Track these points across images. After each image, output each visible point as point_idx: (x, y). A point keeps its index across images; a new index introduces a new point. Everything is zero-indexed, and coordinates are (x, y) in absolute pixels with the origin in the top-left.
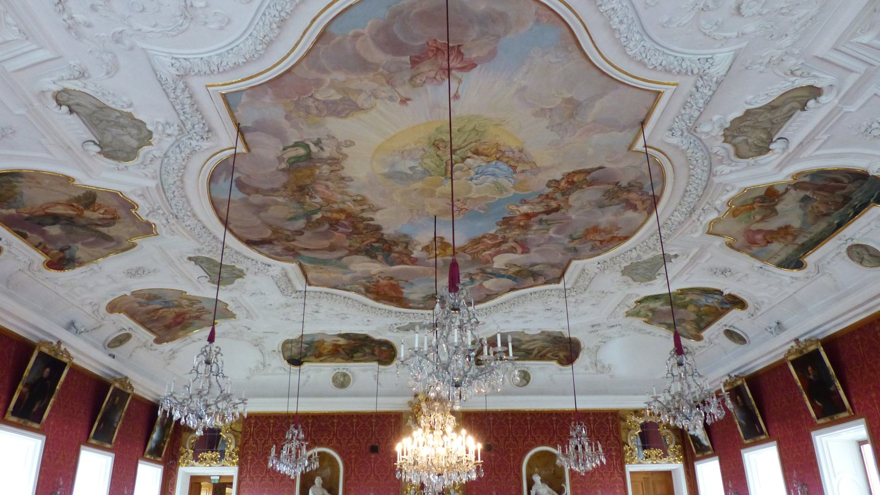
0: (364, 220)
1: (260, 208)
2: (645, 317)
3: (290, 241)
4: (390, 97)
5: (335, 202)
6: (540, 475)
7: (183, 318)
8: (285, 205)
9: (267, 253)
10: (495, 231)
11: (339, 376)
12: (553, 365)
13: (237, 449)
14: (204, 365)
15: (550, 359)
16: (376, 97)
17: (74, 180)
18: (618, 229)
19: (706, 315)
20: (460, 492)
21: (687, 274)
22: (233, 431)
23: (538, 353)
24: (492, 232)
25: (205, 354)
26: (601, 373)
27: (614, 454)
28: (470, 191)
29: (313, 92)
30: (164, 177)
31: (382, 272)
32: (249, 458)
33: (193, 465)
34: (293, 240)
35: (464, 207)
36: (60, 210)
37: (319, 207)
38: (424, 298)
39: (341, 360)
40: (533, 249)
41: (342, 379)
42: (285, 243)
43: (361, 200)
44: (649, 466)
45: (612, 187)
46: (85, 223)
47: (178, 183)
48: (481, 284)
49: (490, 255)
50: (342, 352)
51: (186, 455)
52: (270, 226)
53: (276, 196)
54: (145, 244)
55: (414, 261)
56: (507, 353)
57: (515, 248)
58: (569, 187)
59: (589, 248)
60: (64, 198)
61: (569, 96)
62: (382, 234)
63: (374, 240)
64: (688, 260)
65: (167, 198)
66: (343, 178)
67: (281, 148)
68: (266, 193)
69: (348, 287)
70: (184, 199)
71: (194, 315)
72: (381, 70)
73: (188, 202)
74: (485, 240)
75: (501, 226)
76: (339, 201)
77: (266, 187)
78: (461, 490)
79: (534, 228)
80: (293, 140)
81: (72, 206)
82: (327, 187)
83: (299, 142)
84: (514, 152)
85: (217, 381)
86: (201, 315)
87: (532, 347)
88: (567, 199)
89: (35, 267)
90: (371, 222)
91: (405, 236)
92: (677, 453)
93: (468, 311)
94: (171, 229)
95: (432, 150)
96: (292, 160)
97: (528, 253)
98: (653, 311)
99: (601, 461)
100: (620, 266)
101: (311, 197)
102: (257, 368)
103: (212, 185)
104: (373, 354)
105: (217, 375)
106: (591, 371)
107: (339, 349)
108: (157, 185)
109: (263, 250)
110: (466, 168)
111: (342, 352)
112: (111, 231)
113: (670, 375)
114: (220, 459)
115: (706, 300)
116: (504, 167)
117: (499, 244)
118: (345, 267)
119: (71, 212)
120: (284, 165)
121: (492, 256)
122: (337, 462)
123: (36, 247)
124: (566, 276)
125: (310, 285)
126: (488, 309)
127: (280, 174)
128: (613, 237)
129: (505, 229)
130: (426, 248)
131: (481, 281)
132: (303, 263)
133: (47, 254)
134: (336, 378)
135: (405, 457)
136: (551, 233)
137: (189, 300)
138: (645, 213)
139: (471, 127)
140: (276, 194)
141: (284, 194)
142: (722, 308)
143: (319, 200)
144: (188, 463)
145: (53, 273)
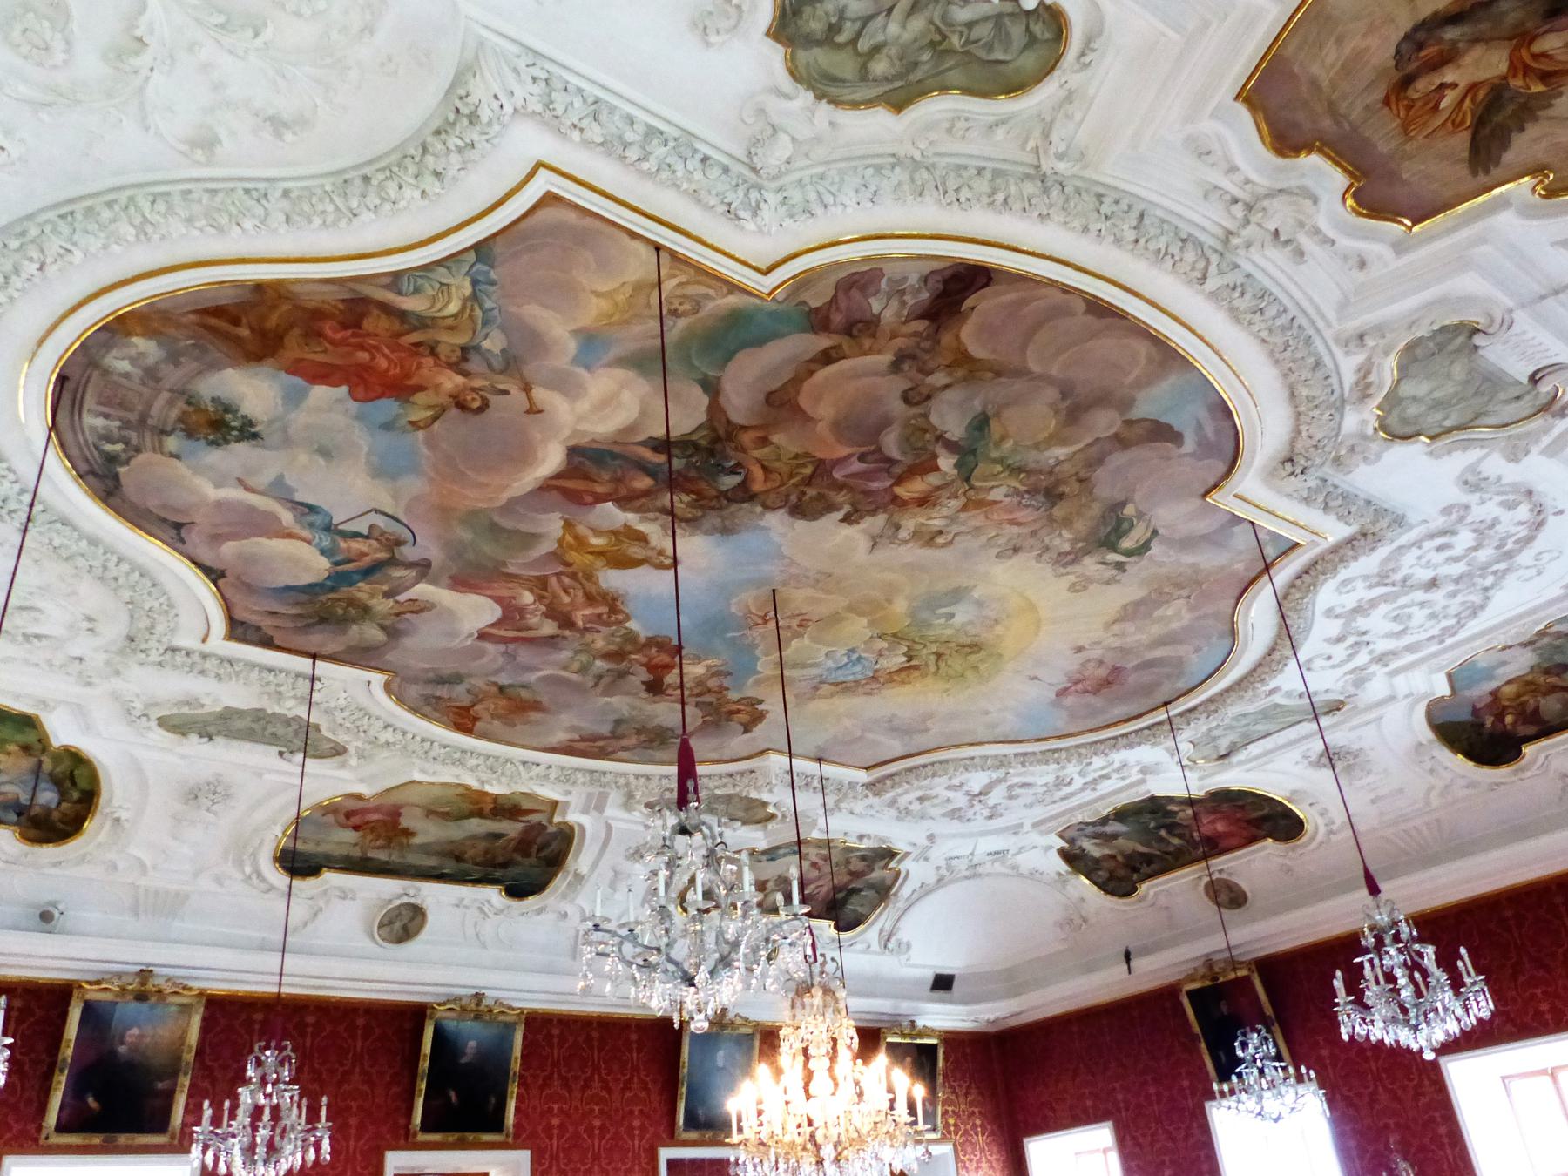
1: (1074, 409)
34: (896, 367)
42: (899, 342)
53: (1075, 453)
67: (1161, 531)
76: (962, 515)
80: (1156, 549)
90: (840, 515)
96: (1126, 525)
120: (1129, 510)
127: (1119, 497)
143: (995, 495)
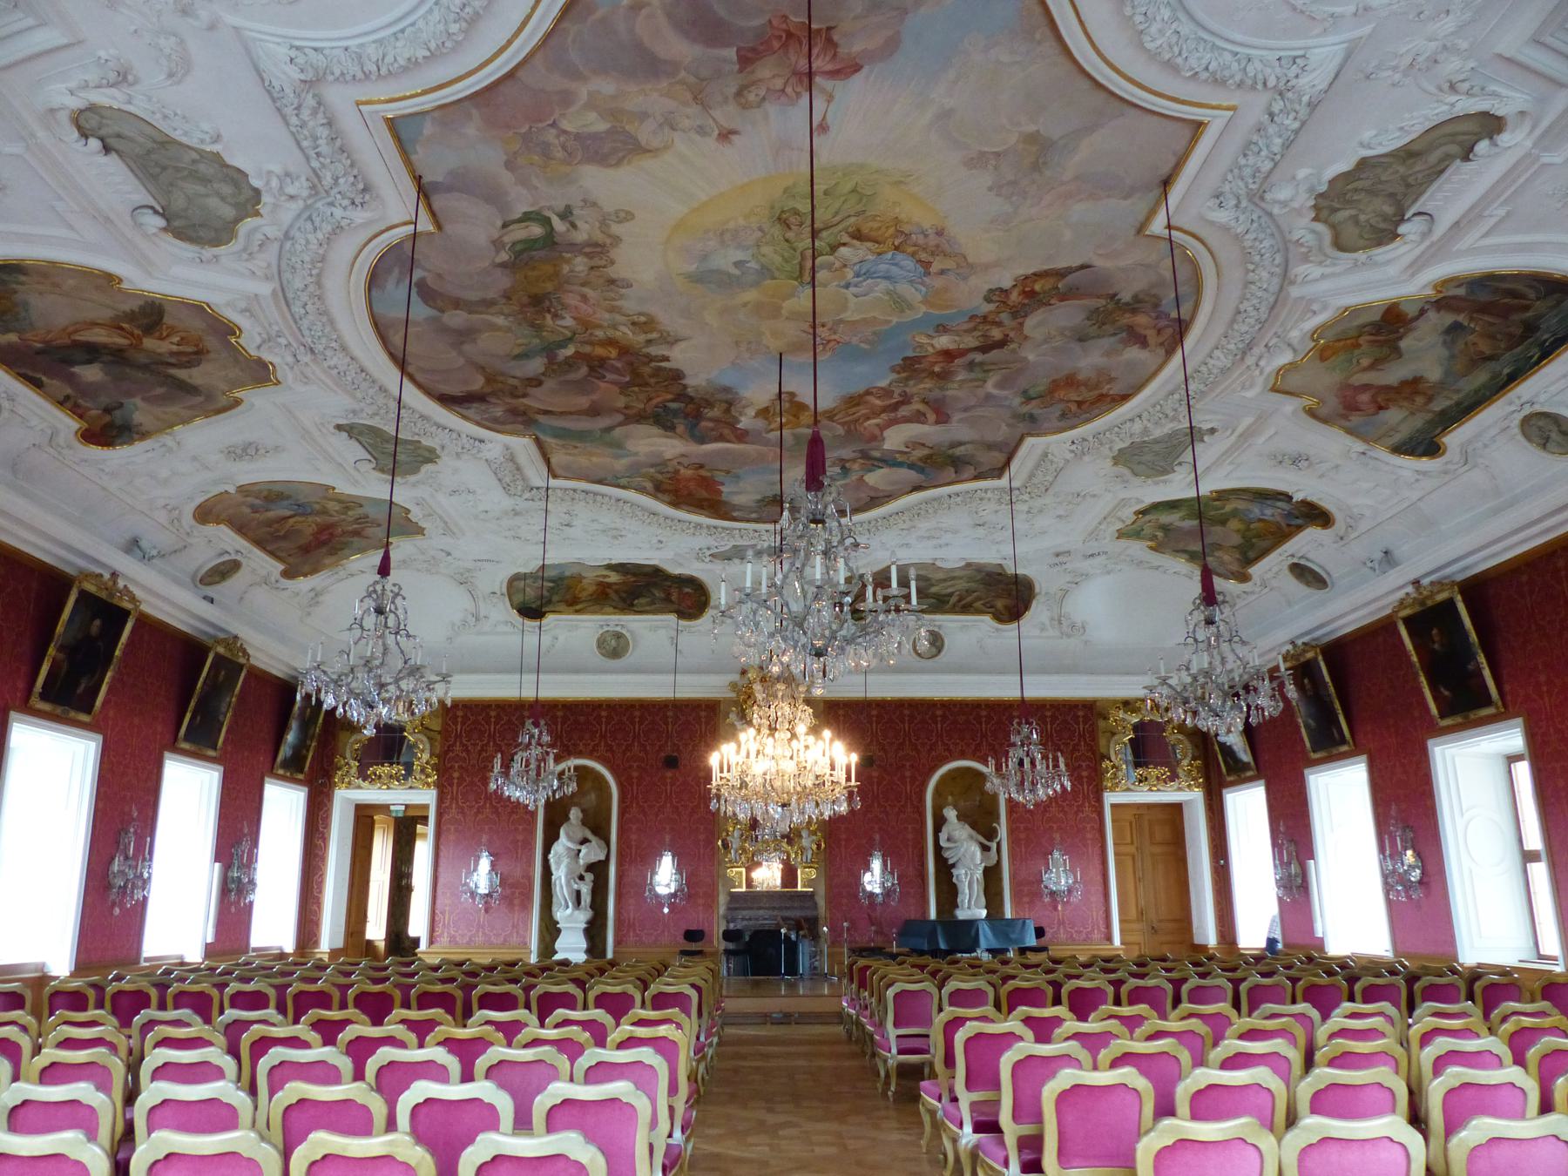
0: (651, 361)
1: (464, 336)
2: (1151, 540)
3: (518, 397)
4: (699, 127)
5: (600, 327)
6: (955, 807)
7: (331, 534)
8: (509, 330)
9: (478, 418)
10: (888, 382)
12: (983, 625)
13: (434, 761)
14: (373, 615)
15: (979, 612)
16: (673, 129)
17: (120, 280)
18: (1111, 380)
19: (1259, 536)
21: (1231, 463)
22: (425, 729)
23: (959, 601)
24: (883, 383)
25: (374, 596)
26: (1069, 636)
27: (1085, 774)
28: (844, 308)
29: (556, 116)
30: (287, 275)
31: (683, 455)
32: (456, 775)
33: (359, 787)
34: (524, 396)
35: (833, 337)
36: (99, 336)
37: (569, 334)
38: (759, 501)
39: (611, 609)
40: (956, 417)
41: (613, 643)
43: (645, 323)
44: (1144, 796)
45: (1103, 302)
46: (147, 361)
47: (311, 288)
48: (861, 479)
49: (878, 425)
50: (613, 595)
51: (345, 769)
52: (482, 369)
54: (256, 399)
55: (742, 436)
56: (907, 598)
57: (924, 415)
58: (1026, 301)
59: (1058, 413)
60: (105, 314)
61: (1032, 128)
62: (685, 387)
63: (670, 397)
64: (1233, 438)
65: (292, 315)
66: (612, 282)
67: (499, 223)
68: (470, 307)
69: (623, 481)
70: (324, 319)
71: (350, 528)
72: (683, 74)
73: (332, 322)
74: (871, 399)
75: (899, 373)
76: (606, 324)
77: (472, 296)
79: (960, 378)
80: (520, 209)
81: (122, 329)
82: (584, 298)
83: (532, 212)
84: (926, 236)
85: (397, 643)
86: (363, 529)
87: (950, 590)
88: (1021, 324)
89: (61, 440)
90: (664, 364)
91: (727, 390)
92: (1194, 773)
93: (840, 525)
94: (302, 373)
95: (777, 231)
96: (518, 247)
97: (946, 422)
98: (1166, 528)
99: (1062, 785)
100: (1110, 449)
101: (556, 316)
102: (465, 623)
103: (374, 293)
104: (668, 599)
105: (397, 633)
106: (1051, 632)
107: (609, 591)
108: (274, 292)
109: (470, 413)
110: (837, 264)
111: (613, 595)
112: (195, 376)
113: (1190, 641)
114: (406, 778)
115: (1261, 511)
116: (909, 263)
117: (895, 407)
118: (618, 445)
119: (120, 341)
120: (504, 256)
121: (882, 428)
122: (607, 782)
123: (62, 403)
124: (1014, 465)
125: (555, 477)
126: (873, 523)
127: (499, 271)
128: (1102, 395)
129: (907, 379)
130: (764, 413)
131: (861, 473)
132: (542, 437)
133: (81, 417)
134: (605, 641)
135: (725, 774)
136: (990, 387)
137: (340, 501)
138: (1162, 352)
139: (849, 186)
140: (492, 310)
141: (506, 311)
142: (1289, 525)
143: (568, 322)
144: (349, 783)
145: (95, 452)
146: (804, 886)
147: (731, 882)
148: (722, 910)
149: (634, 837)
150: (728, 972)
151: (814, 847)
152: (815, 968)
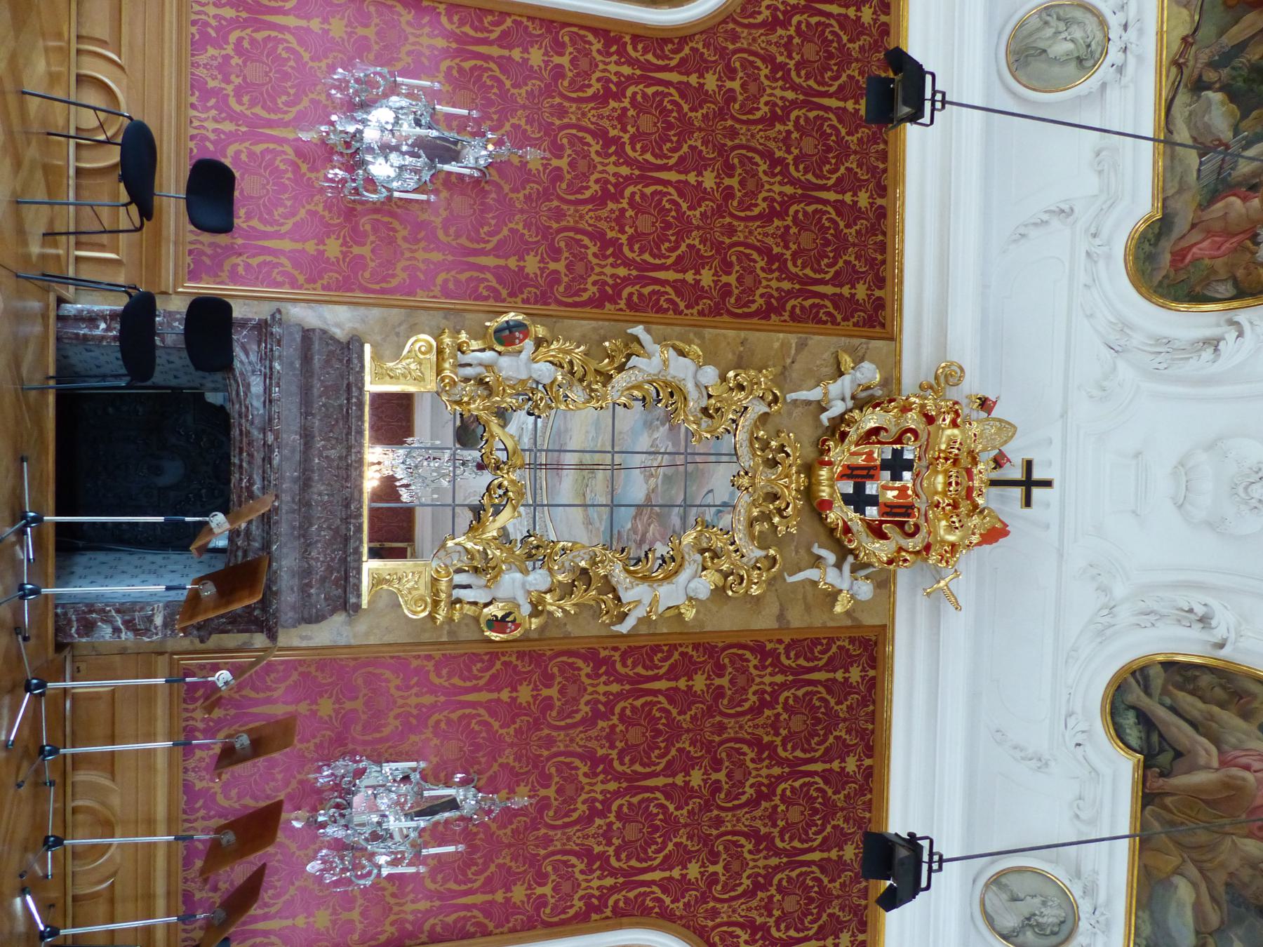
11: (1078, 34)
20: (535, 623)
41: (1061, 48)
78: (542, 628)
134: (1068, 22)
146: (378, 581)
147: (393, 345)
148: (304, 314)
149: (536, 57)
150: (79, 318)
151: (496, 611)
152: (88, 627)
